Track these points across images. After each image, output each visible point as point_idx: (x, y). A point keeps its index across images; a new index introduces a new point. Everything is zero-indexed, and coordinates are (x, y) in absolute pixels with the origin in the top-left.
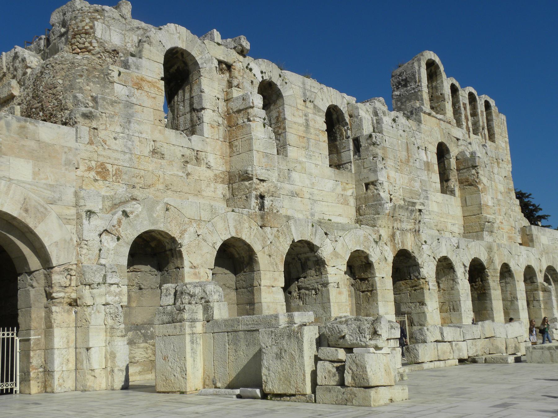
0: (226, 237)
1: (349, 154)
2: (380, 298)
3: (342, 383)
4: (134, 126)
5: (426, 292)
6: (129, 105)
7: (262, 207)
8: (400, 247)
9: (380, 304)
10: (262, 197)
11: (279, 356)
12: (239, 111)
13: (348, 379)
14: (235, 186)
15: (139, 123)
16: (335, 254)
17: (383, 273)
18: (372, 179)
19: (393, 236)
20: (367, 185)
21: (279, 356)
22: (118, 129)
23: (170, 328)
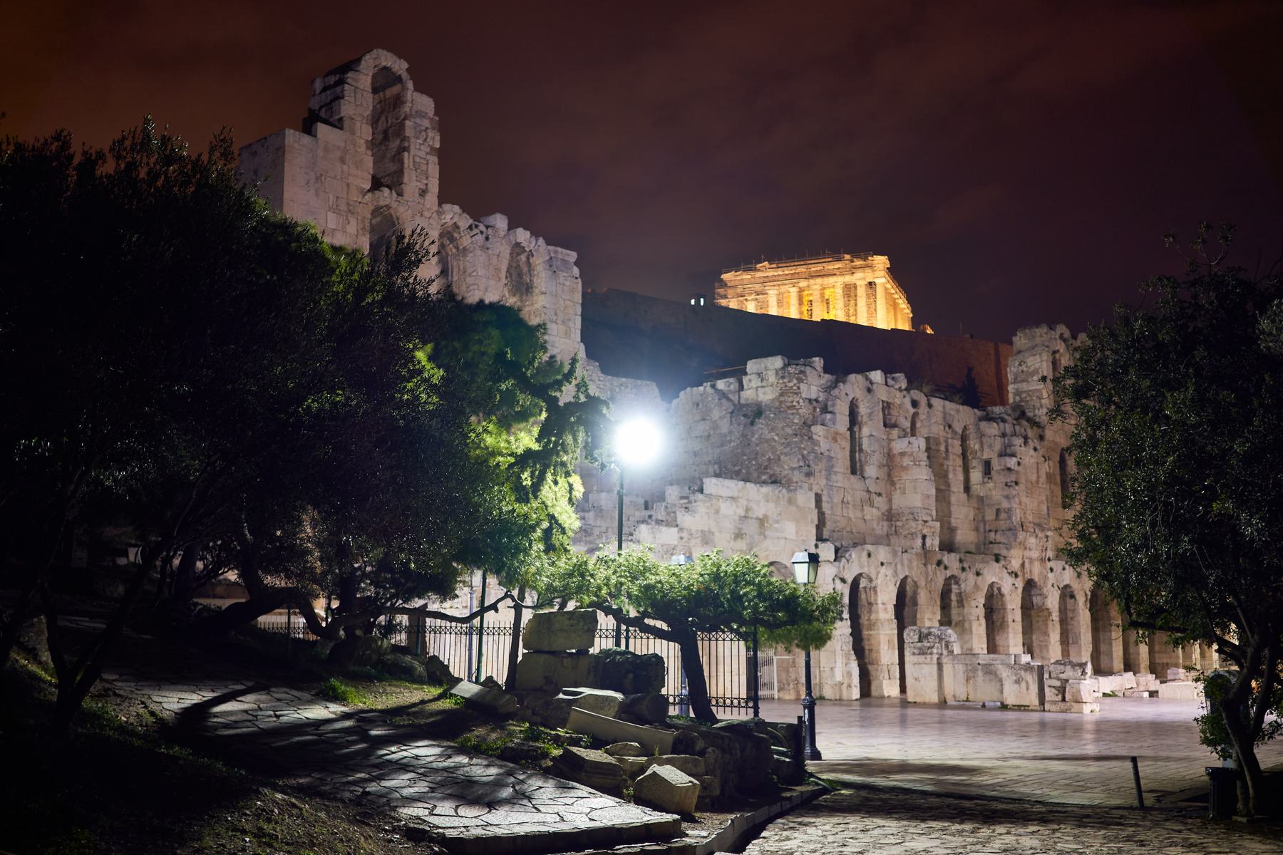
0: (902, 577)
1: (976, 476)
2: (1010, 630)
3: (1064, 699)
4: (833, 477)
5: (1050, 623)
6: (830, 458)
7: (924, 544)
8: (1028, 576)
9: (1011, 635)
10: (924, 537)
11: (1018, 682)
12: (903, 454)
13: (1068, 697)
14: (899, 524)
15: (836, 473)
16: (976, 587)
17: (1013, 604)
18: (1005, 505)
19: (1023, 565)
20: (998, 511)
21: (1018, 682)
22: (824, 482)
23: (921, 659)
